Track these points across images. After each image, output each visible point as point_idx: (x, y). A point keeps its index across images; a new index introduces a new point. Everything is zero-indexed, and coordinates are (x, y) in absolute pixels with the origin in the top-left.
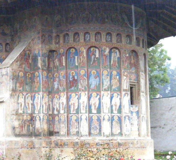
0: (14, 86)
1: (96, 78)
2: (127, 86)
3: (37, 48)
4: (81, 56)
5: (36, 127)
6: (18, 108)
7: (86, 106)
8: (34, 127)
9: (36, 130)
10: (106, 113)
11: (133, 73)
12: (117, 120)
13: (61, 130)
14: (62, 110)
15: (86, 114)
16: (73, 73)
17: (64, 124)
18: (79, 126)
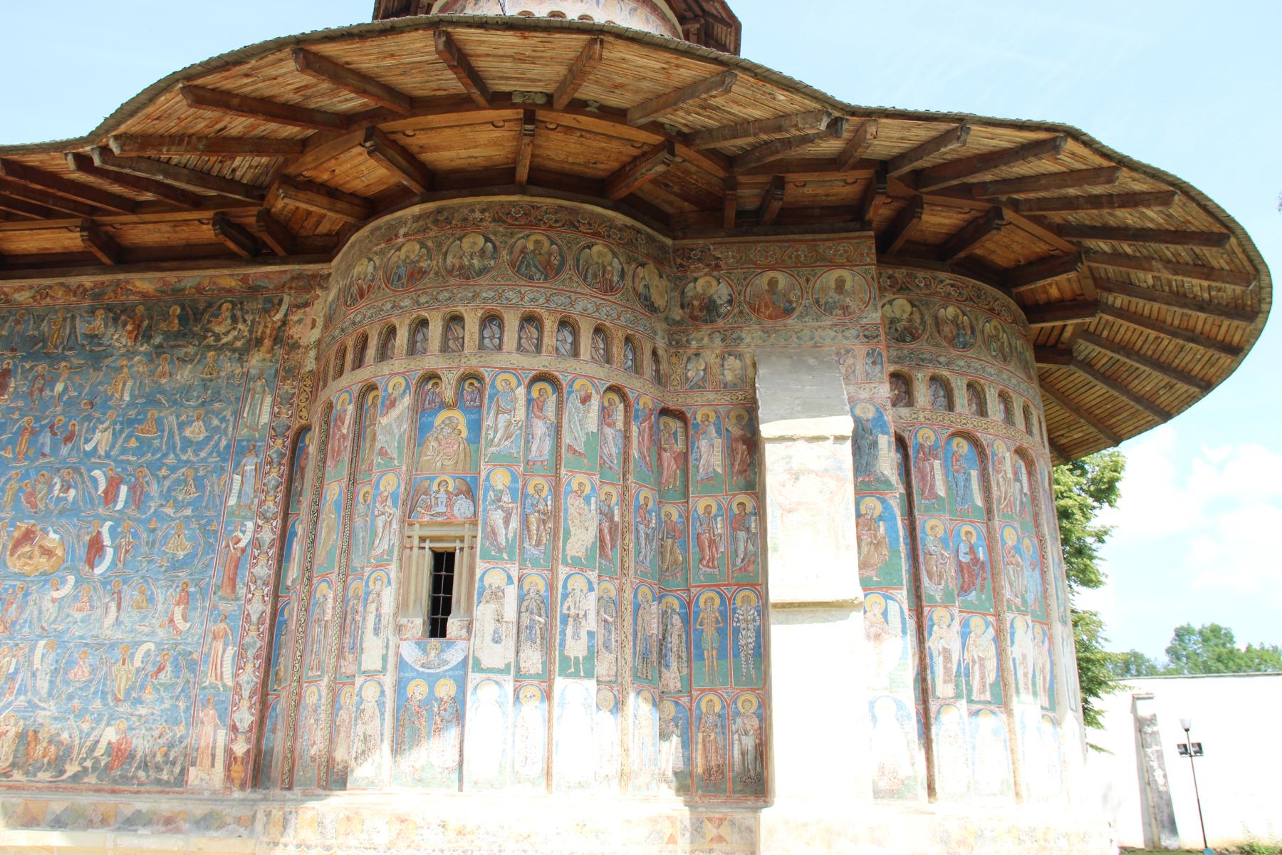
4: (998, 472)
14: (945, 682)
16: (970, 532)
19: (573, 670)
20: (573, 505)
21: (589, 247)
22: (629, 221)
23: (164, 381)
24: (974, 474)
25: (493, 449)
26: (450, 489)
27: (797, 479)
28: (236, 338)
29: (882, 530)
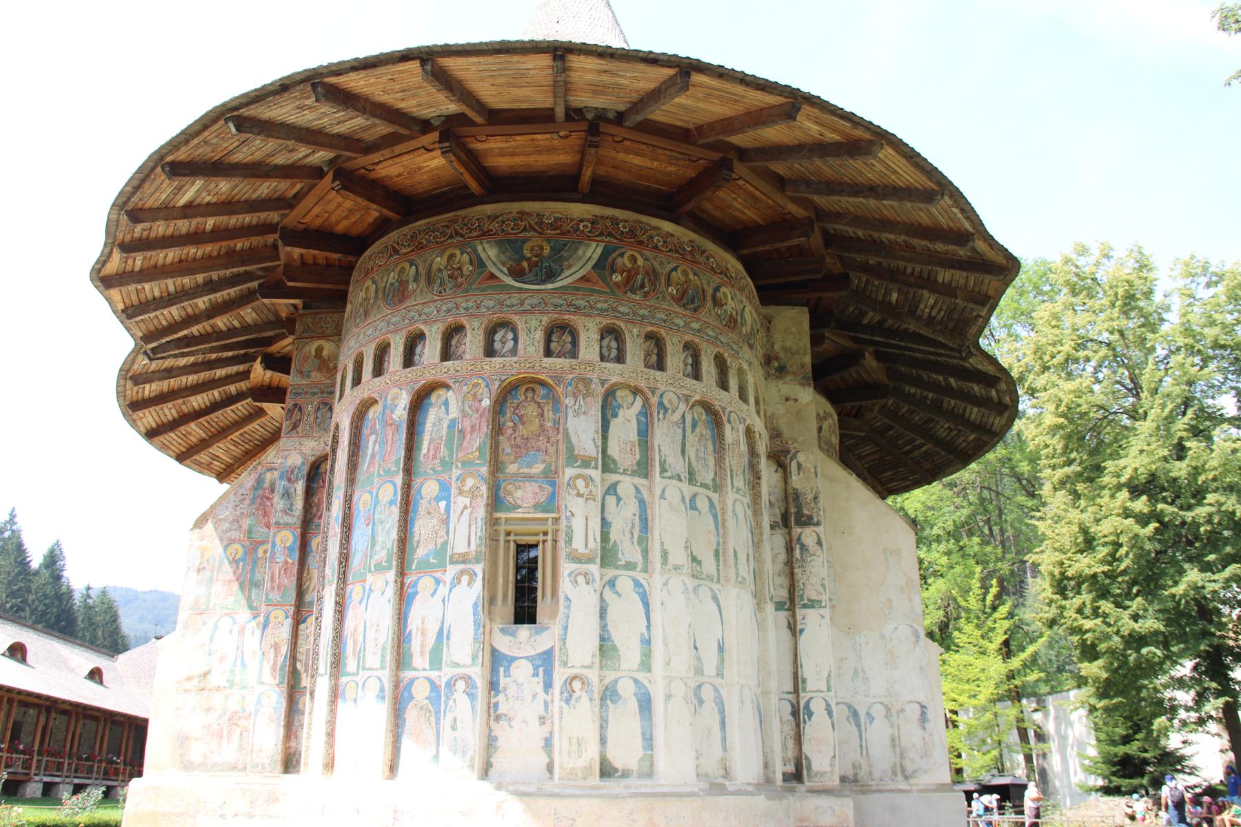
2: (473, 539)
10: (371, 669)
11: (529, 478)
12: (427, 701)
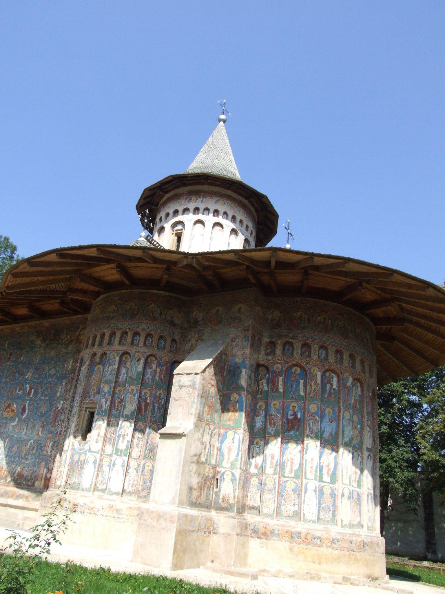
0: (202, 409)
1: (331, 422)
3: (240, 353)
4: (312, 381)
5: (222, 492)
6: (200, 452)
7: (317, 467)
8: (216, 493)
9: (221, 498)
10: (345, 485)
13: (264, 505)
15: (314, 481)
16: (295, 406)
17: (273, 495)
18: (299, 502)
19: (120, 453)
20: (129, 397)
21: (149, 306)
22: (167, 294)
23: (47, 355)
24: (302, 382)
25: (106, 378)
26: (95, 392)
27: (181, 389)
28: (67, 340)
29: (237, 406)
